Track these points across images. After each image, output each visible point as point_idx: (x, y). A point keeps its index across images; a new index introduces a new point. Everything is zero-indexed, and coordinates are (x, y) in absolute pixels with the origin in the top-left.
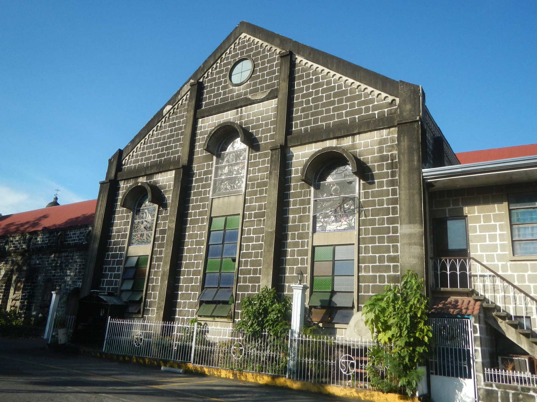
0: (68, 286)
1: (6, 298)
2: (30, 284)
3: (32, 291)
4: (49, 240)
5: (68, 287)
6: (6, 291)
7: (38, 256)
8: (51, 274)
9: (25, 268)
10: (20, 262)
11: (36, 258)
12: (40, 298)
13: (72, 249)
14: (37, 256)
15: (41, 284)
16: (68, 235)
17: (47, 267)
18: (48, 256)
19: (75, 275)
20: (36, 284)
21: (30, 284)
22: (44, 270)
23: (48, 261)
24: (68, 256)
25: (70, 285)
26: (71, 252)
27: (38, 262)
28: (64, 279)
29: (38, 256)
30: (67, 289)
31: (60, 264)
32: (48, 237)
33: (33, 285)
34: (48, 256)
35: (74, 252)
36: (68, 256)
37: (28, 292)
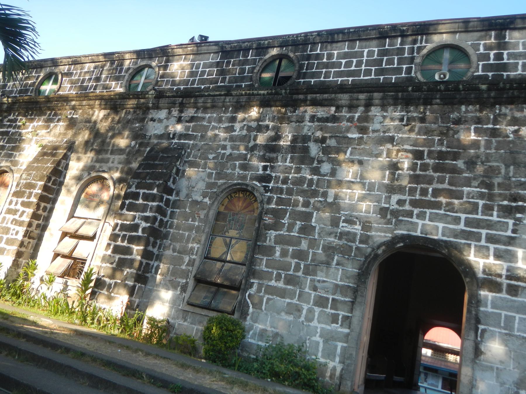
0: (349, 221)
1: (38, 226)
2: (155, 191)
3: (159, 218)
4: (222, 73)
5: (357, 228)
6: (43, 205)
7: (181, 111)
8: (249, 174)
9: (122, 142)
10: (103, 126)
11: (167, 119)
12: (196, 246)
13: (362, 96)
14: (175, 113)
15: (199, 199)
16: (318, 57)
17: (224, 147)
18: (229, 115)
19: (391, 189)
20: (172, 198)
21: (155, 191)
22: (211, 156)
23: (231, 129)
24: (334, 119)
25: (366, 226)
26: (352, 107)
27: (179, 128)
28: (325, 195)
29: (181, 111)
30: (350, 236)
31: (294, 140)
32: (218, 64)
33: (165, 196)
34: (229, 115)
35: (368, 105)
36: (334, 119)
37: (146, 219)
